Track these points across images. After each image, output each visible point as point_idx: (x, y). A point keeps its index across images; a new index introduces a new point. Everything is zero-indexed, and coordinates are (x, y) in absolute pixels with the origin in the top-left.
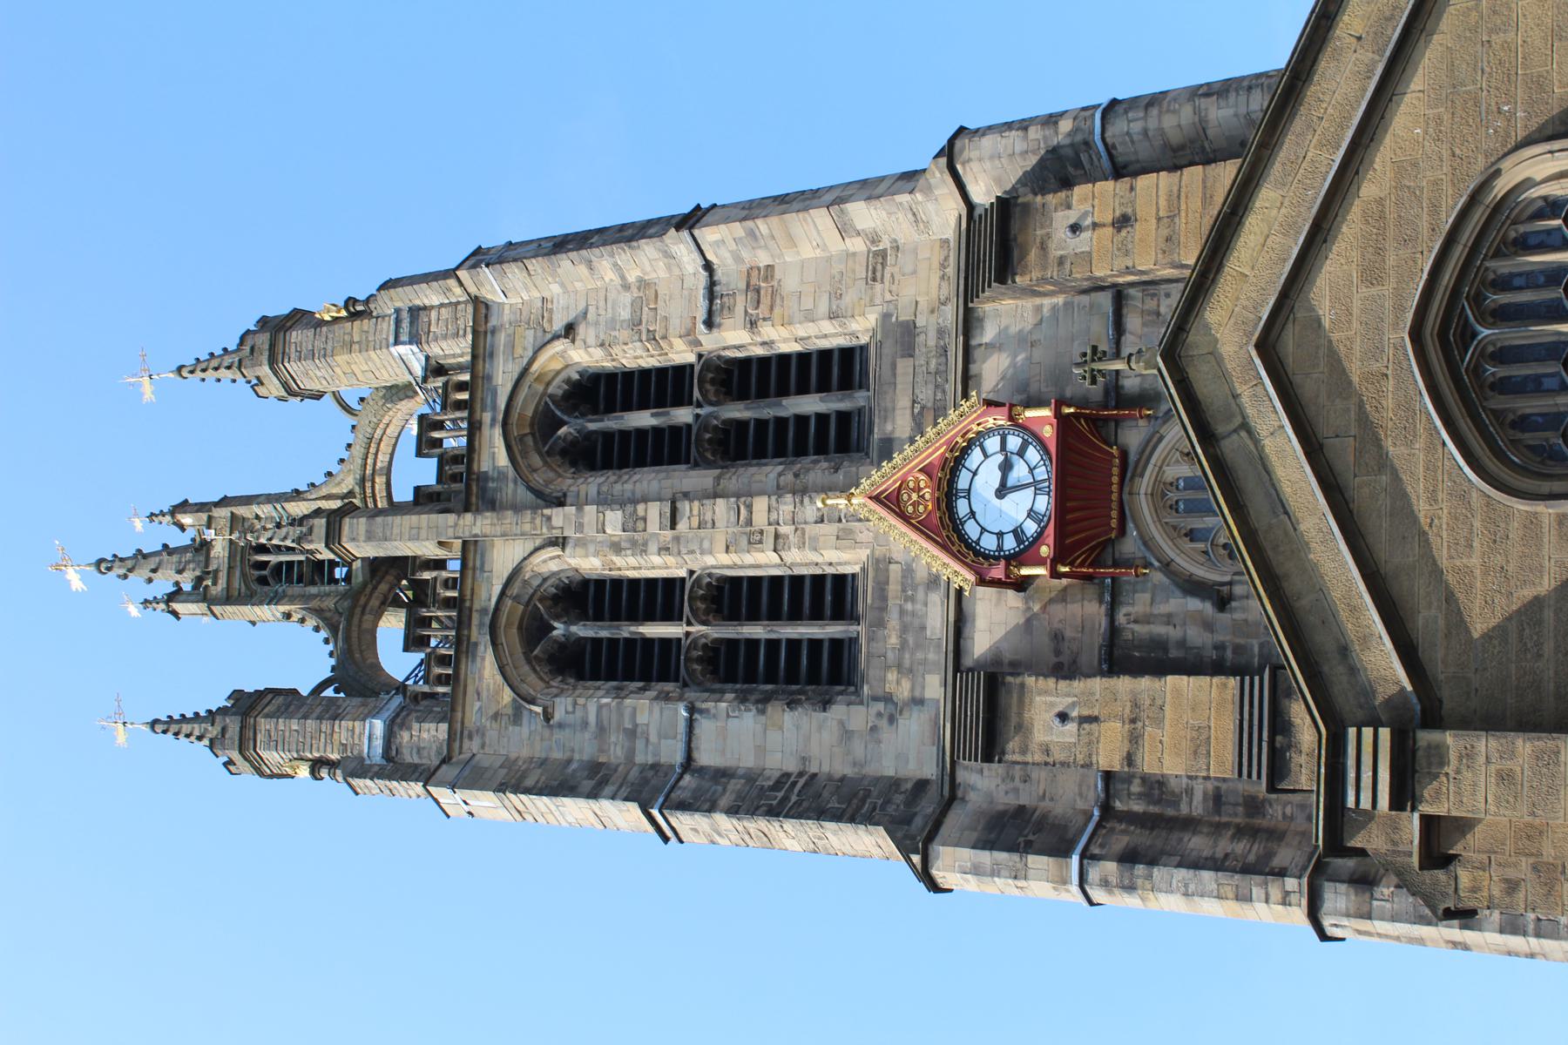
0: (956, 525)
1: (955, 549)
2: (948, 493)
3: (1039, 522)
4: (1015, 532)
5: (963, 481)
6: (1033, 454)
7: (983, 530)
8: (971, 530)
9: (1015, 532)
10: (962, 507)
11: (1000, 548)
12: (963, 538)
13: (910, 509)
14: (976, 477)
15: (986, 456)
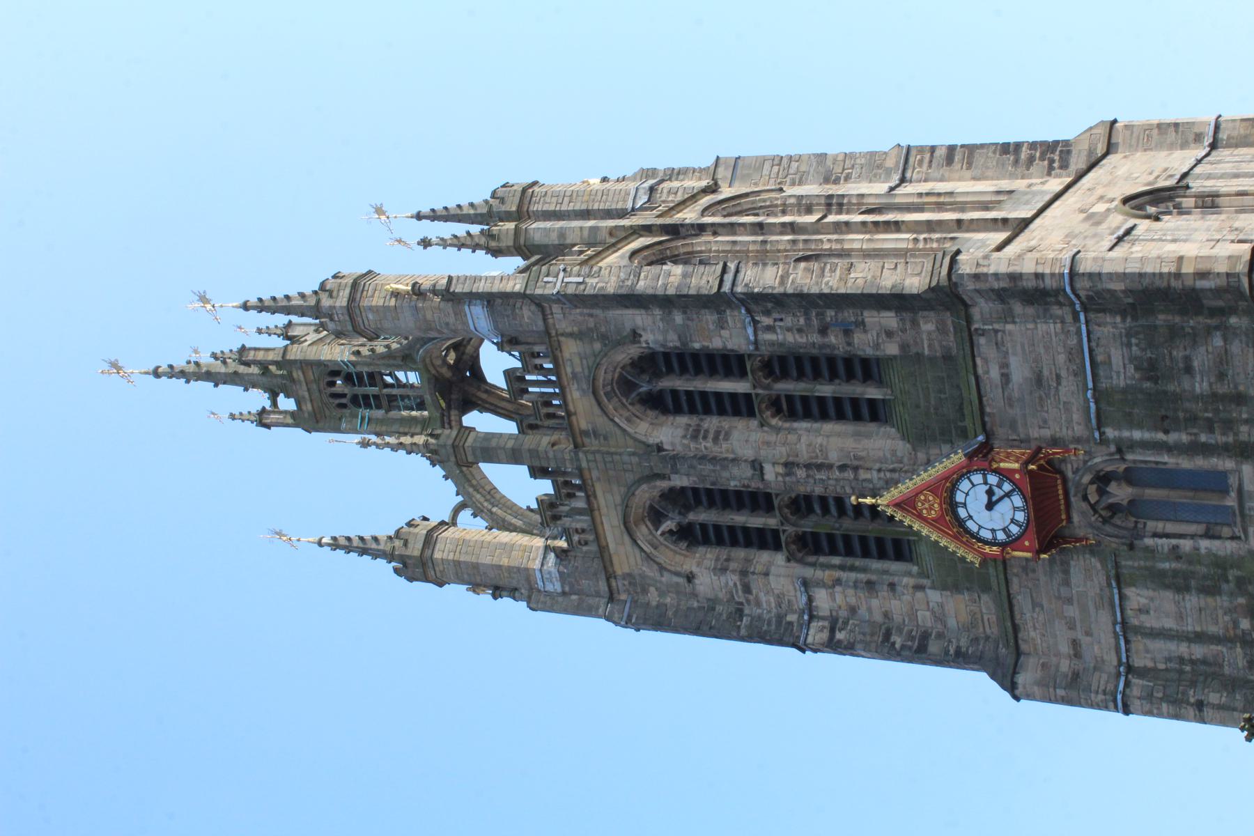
0: (961, 523)
1: (964, 539)
2: (952, 506)
3: (1020, 526)
4: (1004, 530)
5: (960, 497)
6: (1007, 487)
7: (980, 527)
8: (970, 524)
9: (1004, 530)
10: (962, 513)
11: (995, 539)
12: (967, 531)
13: (924, 511)
14: (968, 497)
15: (974, 485)
